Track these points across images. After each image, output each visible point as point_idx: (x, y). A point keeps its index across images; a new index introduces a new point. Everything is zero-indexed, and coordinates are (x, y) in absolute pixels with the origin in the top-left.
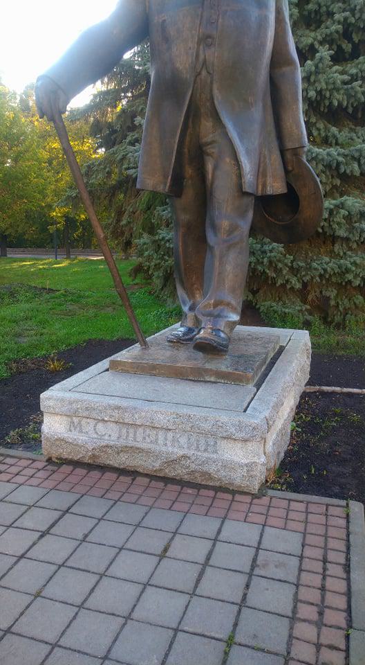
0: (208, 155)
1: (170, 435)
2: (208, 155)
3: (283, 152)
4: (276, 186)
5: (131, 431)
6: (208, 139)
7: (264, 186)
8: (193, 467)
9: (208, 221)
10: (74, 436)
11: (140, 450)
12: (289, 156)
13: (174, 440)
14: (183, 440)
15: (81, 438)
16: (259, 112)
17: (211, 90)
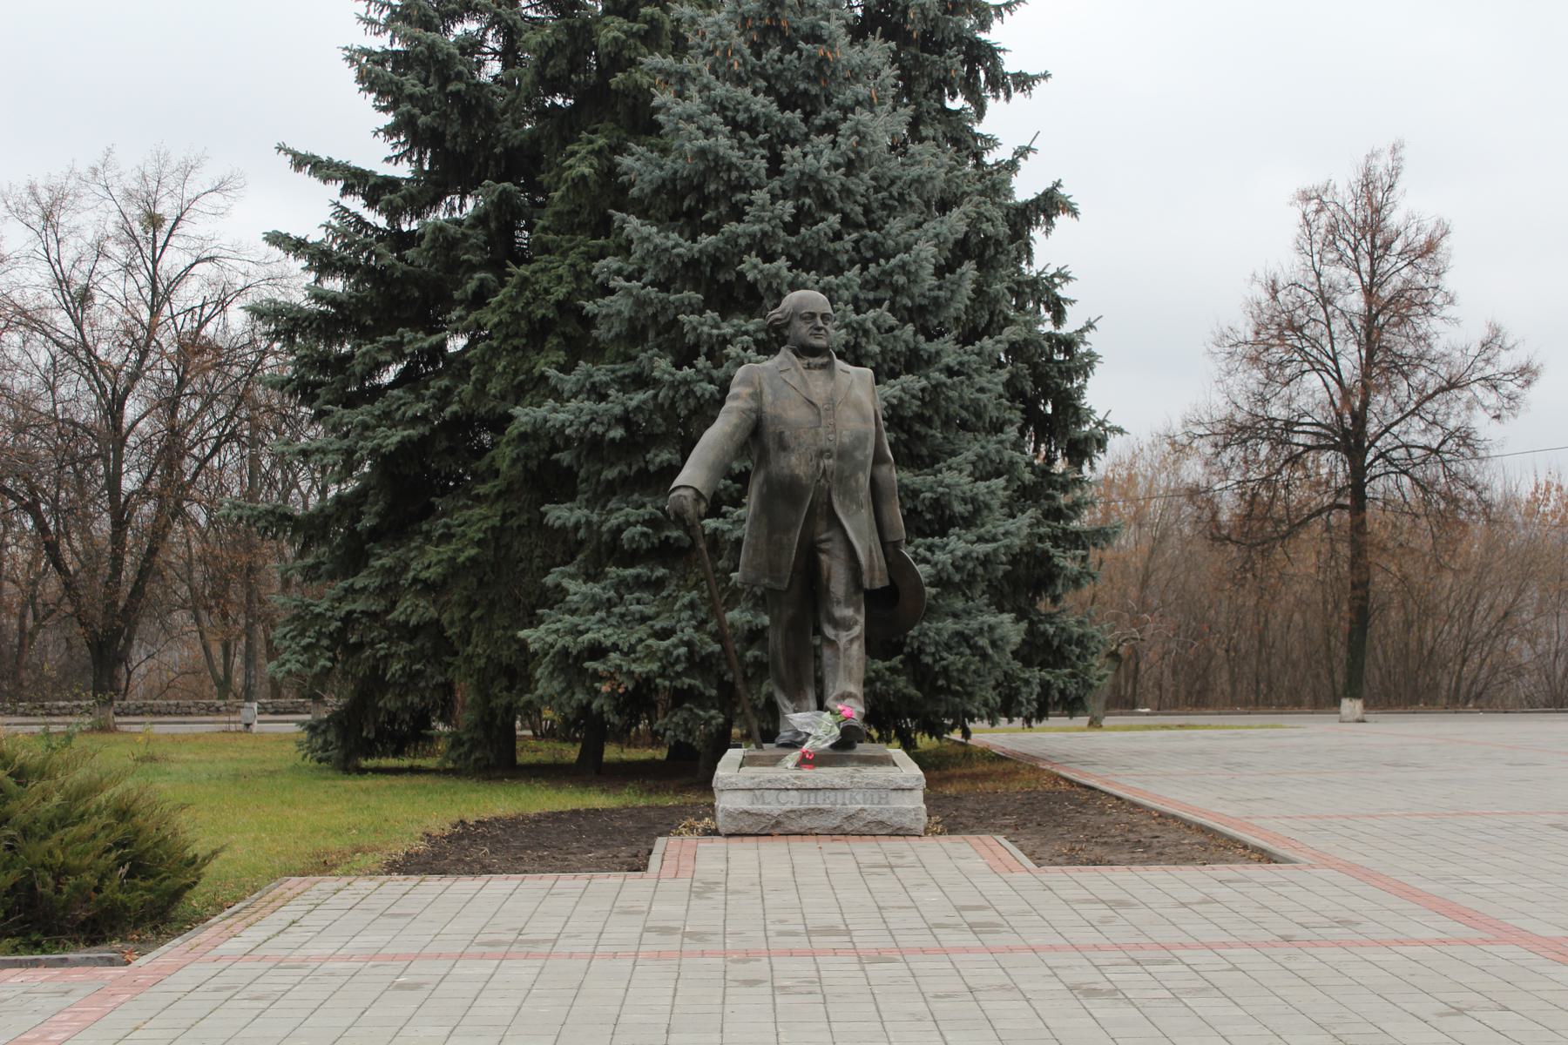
0: (824, 551)
1: (847, 794)
2: (824, 551)
3: (884, 543)
4: (880, 581)
5: (812, 795)
6: (823, 537)
7: (872, 579)
8: (870, 818)
9: (822, 617)
10: (758, 807)
11: (820, 811)
12: (890, 548)
13: (852, 798)
14: (859, 797)
15: (765, 808)
16: (866, 514)
17: (830, 498)
